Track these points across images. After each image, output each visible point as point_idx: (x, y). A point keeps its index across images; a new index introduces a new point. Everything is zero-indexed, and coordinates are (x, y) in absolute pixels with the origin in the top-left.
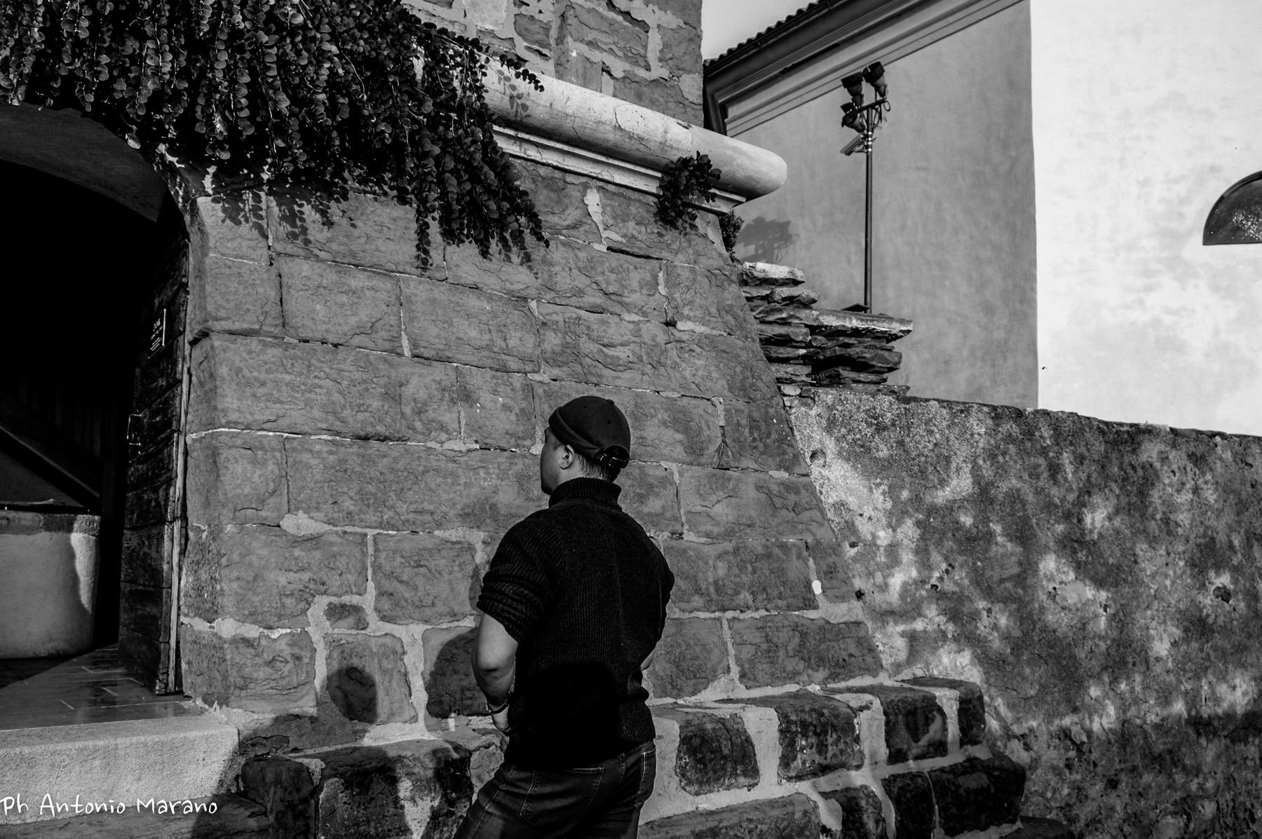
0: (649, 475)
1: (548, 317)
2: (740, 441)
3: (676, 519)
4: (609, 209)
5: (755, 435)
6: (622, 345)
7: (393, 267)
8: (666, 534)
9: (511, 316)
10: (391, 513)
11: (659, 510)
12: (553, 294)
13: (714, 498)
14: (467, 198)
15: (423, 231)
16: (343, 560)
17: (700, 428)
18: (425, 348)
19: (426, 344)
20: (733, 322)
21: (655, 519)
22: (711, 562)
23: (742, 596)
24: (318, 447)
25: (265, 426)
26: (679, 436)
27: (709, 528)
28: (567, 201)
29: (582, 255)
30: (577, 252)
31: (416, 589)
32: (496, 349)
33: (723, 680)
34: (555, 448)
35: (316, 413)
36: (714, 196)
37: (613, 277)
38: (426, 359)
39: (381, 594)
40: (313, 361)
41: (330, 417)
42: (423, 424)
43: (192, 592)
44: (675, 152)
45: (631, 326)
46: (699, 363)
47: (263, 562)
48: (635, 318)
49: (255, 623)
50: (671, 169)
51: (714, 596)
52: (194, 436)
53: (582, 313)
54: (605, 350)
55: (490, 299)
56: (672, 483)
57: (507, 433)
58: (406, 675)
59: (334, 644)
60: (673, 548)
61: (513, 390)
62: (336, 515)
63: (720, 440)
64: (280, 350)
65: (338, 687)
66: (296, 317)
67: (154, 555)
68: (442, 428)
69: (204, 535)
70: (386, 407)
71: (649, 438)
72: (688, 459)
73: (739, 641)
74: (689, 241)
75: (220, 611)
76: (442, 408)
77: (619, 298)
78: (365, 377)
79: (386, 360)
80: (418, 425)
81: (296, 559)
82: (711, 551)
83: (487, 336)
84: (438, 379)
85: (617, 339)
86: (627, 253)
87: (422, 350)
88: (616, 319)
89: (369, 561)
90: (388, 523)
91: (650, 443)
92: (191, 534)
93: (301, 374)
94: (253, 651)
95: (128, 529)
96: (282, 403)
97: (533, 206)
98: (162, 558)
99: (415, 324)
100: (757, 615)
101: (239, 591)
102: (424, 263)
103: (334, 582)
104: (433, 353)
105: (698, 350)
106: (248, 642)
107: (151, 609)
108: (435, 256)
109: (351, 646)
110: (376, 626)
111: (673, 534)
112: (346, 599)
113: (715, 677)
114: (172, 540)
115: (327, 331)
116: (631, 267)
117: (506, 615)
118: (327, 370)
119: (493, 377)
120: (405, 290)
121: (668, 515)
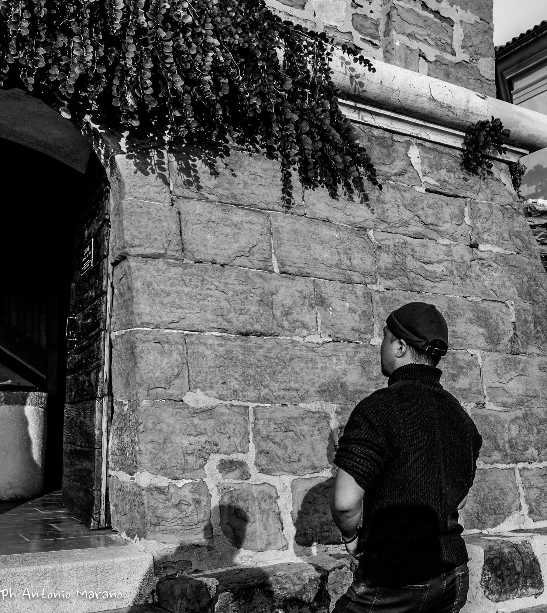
0: (460, 360)
1: (382, 242)
2: (527, 333)
3: (480, 393)
4: (426, 160)
5: (538, 328)
6: (438, 262)
7: (265, 206)
8: (473, 404)
9: (354, 242)
10: (266, 391)
11: (467, 386)
12: (385, 225)
13: (508, 377)
14: (320, 154)
15: (287, 178)
16: (231, 426)
17: (497, 323)
18: (290, 266)
19: (290, 264)
20: (520, 244)
21: (464, 393)
22: (506, 426)
23: (529, 451)
24: (210, 341)
25: (170, 326)
26: (482, 330)
27: (505, 399)
28: (394, 155)
29: (407, 195)
30: (403, 193)
31: (286, 448)
32: (343, 267)
33: (516, 515)
34: (392, 342)
35: (209, 316)
36: (505, 150)
37: (430, 211)
38: (290, 274)
39: (260, 452)
40: (206, 277)
41: (220, 319)
42: (290, 323)
43: (117, 452)
44: (475, 117)
45: (445, 248)
46: (496, 275)
47: (171, 429)
48: (448, 242)
49: (165, 475)
50: (473, 130)
51: (509, 451)
52: (117, 333)
53: (408, 239)
54: (425, 266)
55: (338, 229)
56: (477, 365)
57: (353, 329)
58: (279, 514)
59: (225, 491)
60: (478, 415)
61: (357, 297)
62: (225, 392)
63: (512, 333)
64: (181, 269)
65: (228, 524)
66: (191, 244)
67: (89, 423)
68: (304, 326)
69: (126, 408)
70: (261, 311)
71: (459, 332)
72: (489, 347)
73: (527, 485)
74: (487, 184)
75: (139, 466)
76: (304, 311)
77: (435, 228)
78: (245, 288)
79: (261, 276)
80: (286, 324)
81: (195, 426)
82: (507, 417)
83: (337, 257)
84: (300, 289)
85: (434, 258)
86: (441, 193)
87: (288, 268)
88: (433, 243)
89: (250, 427)
90: (264, 398)
91: (460, 335)
92: (116, 407)
93: (196, 287)
94: (163, 496)
95: (68, 403)
96: (183, 308)
97: (369, 159)
98: (94, 425)
99: (282, 248)
100: (541, 465)
101: (153, 451)
102: (288, 203)
103: (224, 444)
104: (296, 270)
105: (495, 265)
106: (160, 490)
107: (86, 465)
108: (297, 197)
109: (238, 492)
110: (256, 476)
111: (478, 404)
112: (234, 456)
113: (510, 513)
114: (102, 412)
115: (216, 254)
116: (444, 204)
117: (355, 469)
118: (216, 283)
119: (342, 288)
120: (274, 223)
121: (474, 390)
